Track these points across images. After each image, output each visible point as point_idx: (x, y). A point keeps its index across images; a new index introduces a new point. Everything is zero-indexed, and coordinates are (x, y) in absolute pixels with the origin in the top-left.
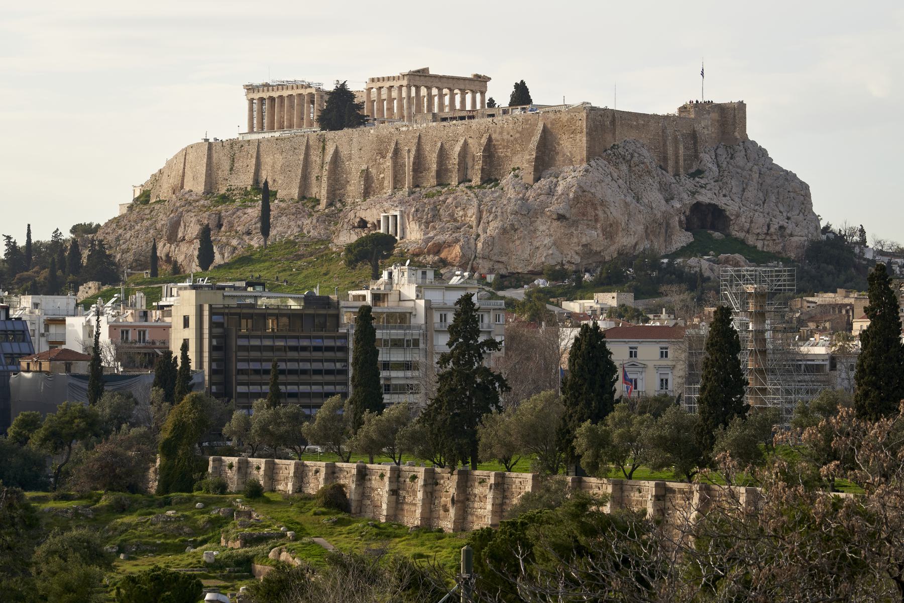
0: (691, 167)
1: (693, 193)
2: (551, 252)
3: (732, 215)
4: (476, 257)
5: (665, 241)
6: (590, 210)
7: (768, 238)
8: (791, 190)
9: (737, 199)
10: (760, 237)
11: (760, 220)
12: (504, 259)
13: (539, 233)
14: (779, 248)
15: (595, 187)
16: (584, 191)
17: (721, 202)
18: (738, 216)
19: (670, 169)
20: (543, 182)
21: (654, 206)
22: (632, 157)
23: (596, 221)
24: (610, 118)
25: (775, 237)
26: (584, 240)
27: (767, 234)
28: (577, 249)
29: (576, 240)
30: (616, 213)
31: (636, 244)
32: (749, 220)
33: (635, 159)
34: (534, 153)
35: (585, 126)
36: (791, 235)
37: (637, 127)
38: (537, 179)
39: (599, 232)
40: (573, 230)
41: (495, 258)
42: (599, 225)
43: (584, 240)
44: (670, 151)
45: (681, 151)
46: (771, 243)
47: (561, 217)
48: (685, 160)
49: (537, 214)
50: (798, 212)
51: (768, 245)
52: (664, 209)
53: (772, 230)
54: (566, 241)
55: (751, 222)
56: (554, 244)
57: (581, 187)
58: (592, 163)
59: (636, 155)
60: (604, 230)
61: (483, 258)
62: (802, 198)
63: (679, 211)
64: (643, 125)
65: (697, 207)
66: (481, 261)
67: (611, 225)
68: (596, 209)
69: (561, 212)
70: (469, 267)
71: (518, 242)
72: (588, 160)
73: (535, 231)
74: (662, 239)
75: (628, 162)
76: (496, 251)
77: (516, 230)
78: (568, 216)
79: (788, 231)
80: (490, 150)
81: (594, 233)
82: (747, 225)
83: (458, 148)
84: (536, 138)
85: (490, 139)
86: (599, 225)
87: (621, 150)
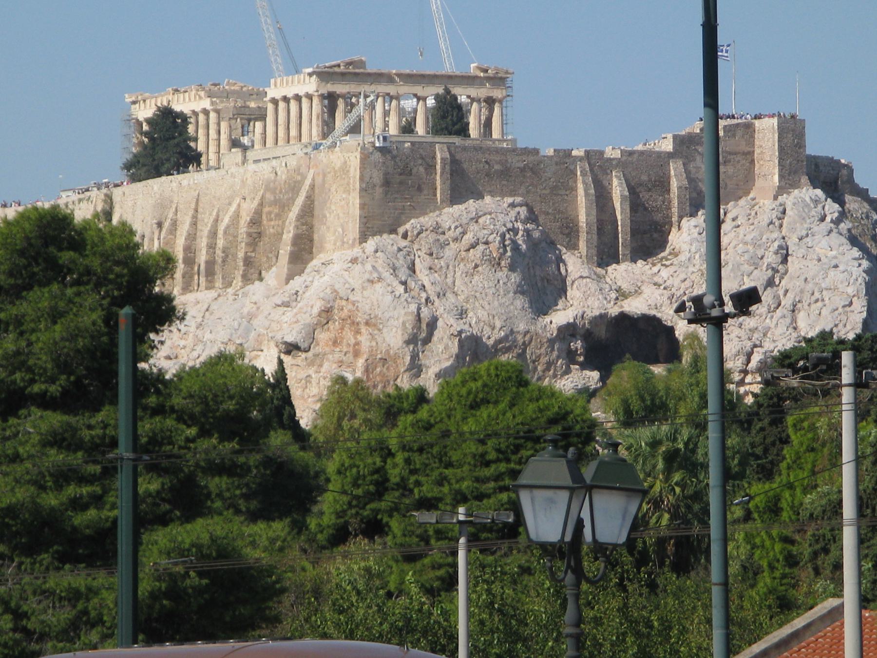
1: (622, 295)
6: (349, 336)
20: (297, 283)
23: (357, 354)
34: (291, 228)
35: (358, 177)
38: (290, 278)
40: (311, 371)
58: (371, 244)
63: (568, 331)
68: (358, 332)
69: (290, 339)
72: (363, 238)
78: (303, 346)
80: (256, 221)
83: (226, 220)
84: (300, 200)
85: (261, 204)
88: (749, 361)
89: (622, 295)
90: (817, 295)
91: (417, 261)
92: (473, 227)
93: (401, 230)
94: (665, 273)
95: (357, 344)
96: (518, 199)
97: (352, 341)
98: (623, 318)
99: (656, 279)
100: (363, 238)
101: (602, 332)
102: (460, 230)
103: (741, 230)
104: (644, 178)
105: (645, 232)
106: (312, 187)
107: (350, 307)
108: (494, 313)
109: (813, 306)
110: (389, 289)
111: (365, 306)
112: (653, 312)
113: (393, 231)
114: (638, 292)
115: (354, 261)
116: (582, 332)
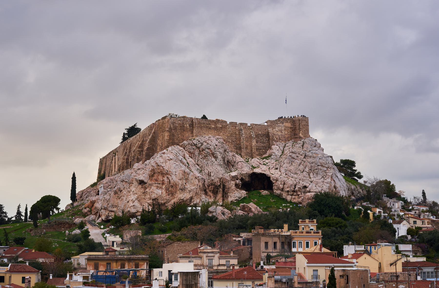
0: (265, 153)
1: (254, 168)
2: (133, 204)
3: (274, 180)
4: (101, 208)
5: (223, 196)
6: (160, 178)
7: (295, 194)
8: (319, 164)
9: (283, 171)
10: (290, 193)
11: (290, 182)
12: (115, 209)
13: (131, 193)
14: (300, 200)
15: (166, 162)
16: (159, 166)
17: (267, 173)
18: (277, 180)
19: (243, 154)
21: (212, 175)
22: (202, 144)
23: (163, 184)
24: (190, 122)
25: (299, 193)
26: (153, 196)
27: (294, 191)
28: (149, 202)
29: (148, 196)
30: (174, 179)
31: (191, 198)
32: (283, 183)
33: (203, 147)
36: (309, 192)
37: (216, 129)
39: (163, 191)
41: (110, 209)
42: (164, 187)
43: (154, 196)
44: (244, 143)
45: (254, 143)
46: (296, 197)
47: (142, 182)
48: (257, 149)
49: (133, 181)
50: (321, 177)
51: (294, 198)
52: (221, 176)
53: (297, 189)
54: (143, 197)
55: (284, 184)
56: (136, 199)
57: (157, 163)
58: (170, 148)
59: (205, 144)
60: (167, 189)
61: (104, 209)
62: (325, 169)
64: (221, 128)
65: (254, 176)
66: (102, 211)
67: (172, 186)
70: (98, 214)
71: (120, 199)
73: (129, 192)
74: (220, 196)
75: (199, 148)
76: (110, 204)
77: (121, 191)
78: (146, 181)
79: (308, 189)
81: (160, 192)
82: (281, 186)
86: (164, 187)
87: (195, 142)
88: (295, 188)
89: (254, 168)
90: (316, 168)
91: (186, 154)
92: (205, 144)
93: (180, 144)
94: (267, 161)
95: (163, 180)
96: (220, 137)
97: (162, 180)
98: (254, 174)
99: (264, 163)
100: (168, 147)
101: (247, 180)
102: (200, 144)
103: (291, 149)
104: (260, 133)
105: (260, 149)
106: (154, 133)
107: (161, 168)
108: (210, 171)
109: (315, 171)
110: (175, 162)
111: (166, 168)
112: (263, 172)
113: (178, 145)
114: (258, 167)
115: (164, 153)
116: (240, 178)
